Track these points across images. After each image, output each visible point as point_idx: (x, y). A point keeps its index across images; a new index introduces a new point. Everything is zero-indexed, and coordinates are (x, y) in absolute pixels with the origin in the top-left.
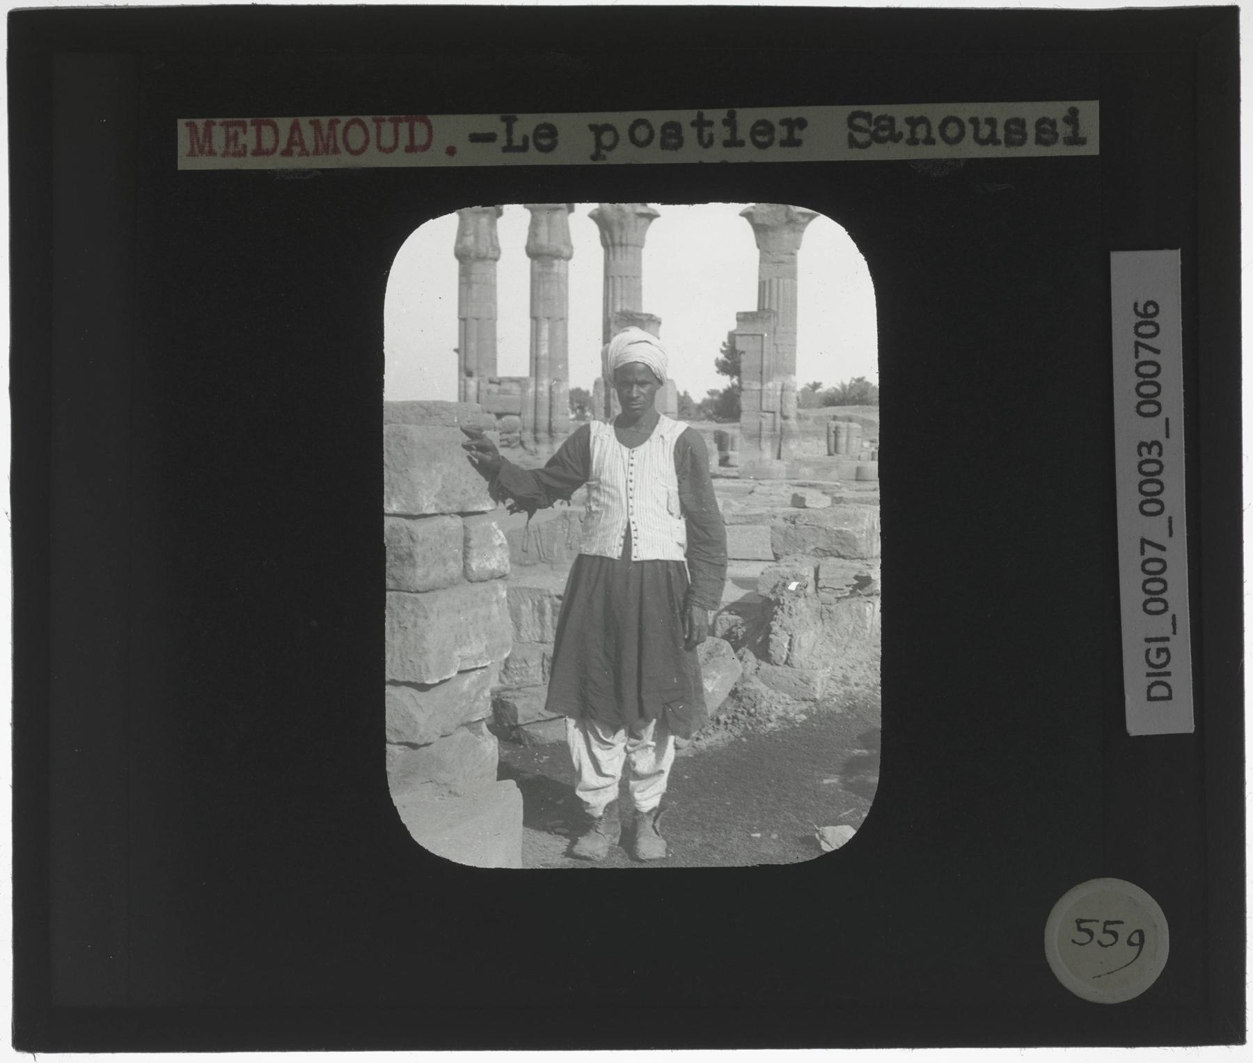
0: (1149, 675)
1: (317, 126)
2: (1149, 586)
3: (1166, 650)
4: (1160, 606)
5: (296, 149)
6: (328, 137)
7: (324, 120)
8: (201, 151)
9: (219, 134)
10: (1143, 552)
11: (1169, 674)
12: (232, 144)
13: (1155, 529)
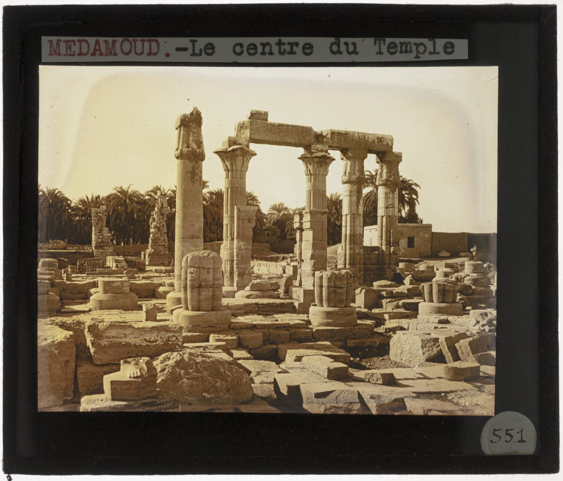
1: (106, 41)
5: (98, 53)
6: (112, 47)
7: (110, 39)
8: (55, 53)
9: (63, 46)
12: (69, 50)
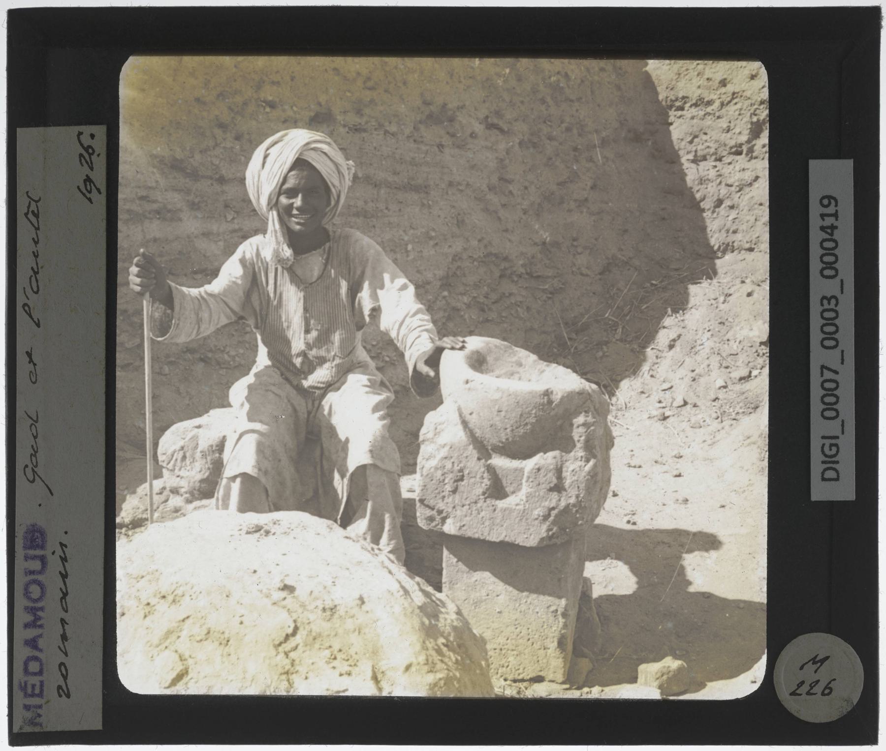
0: (823, 462)
2: (827, 400)
3: (836, 445)
4: (833, 414)
10: (822, 376)
11: (837, 462)
13: (831, 358)
